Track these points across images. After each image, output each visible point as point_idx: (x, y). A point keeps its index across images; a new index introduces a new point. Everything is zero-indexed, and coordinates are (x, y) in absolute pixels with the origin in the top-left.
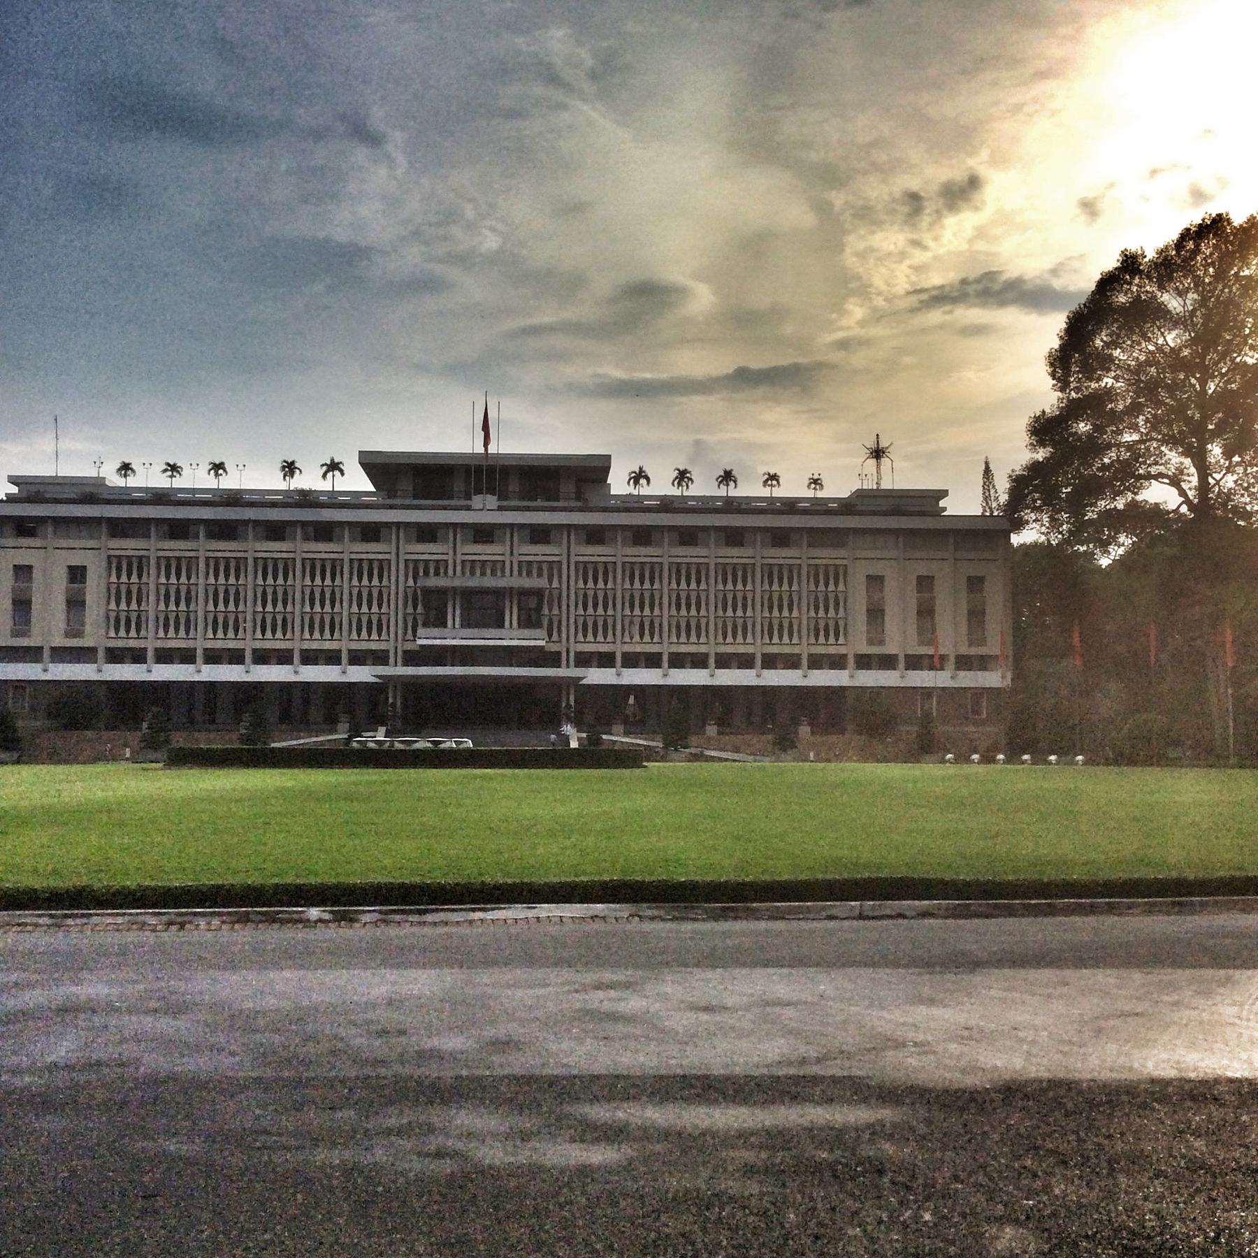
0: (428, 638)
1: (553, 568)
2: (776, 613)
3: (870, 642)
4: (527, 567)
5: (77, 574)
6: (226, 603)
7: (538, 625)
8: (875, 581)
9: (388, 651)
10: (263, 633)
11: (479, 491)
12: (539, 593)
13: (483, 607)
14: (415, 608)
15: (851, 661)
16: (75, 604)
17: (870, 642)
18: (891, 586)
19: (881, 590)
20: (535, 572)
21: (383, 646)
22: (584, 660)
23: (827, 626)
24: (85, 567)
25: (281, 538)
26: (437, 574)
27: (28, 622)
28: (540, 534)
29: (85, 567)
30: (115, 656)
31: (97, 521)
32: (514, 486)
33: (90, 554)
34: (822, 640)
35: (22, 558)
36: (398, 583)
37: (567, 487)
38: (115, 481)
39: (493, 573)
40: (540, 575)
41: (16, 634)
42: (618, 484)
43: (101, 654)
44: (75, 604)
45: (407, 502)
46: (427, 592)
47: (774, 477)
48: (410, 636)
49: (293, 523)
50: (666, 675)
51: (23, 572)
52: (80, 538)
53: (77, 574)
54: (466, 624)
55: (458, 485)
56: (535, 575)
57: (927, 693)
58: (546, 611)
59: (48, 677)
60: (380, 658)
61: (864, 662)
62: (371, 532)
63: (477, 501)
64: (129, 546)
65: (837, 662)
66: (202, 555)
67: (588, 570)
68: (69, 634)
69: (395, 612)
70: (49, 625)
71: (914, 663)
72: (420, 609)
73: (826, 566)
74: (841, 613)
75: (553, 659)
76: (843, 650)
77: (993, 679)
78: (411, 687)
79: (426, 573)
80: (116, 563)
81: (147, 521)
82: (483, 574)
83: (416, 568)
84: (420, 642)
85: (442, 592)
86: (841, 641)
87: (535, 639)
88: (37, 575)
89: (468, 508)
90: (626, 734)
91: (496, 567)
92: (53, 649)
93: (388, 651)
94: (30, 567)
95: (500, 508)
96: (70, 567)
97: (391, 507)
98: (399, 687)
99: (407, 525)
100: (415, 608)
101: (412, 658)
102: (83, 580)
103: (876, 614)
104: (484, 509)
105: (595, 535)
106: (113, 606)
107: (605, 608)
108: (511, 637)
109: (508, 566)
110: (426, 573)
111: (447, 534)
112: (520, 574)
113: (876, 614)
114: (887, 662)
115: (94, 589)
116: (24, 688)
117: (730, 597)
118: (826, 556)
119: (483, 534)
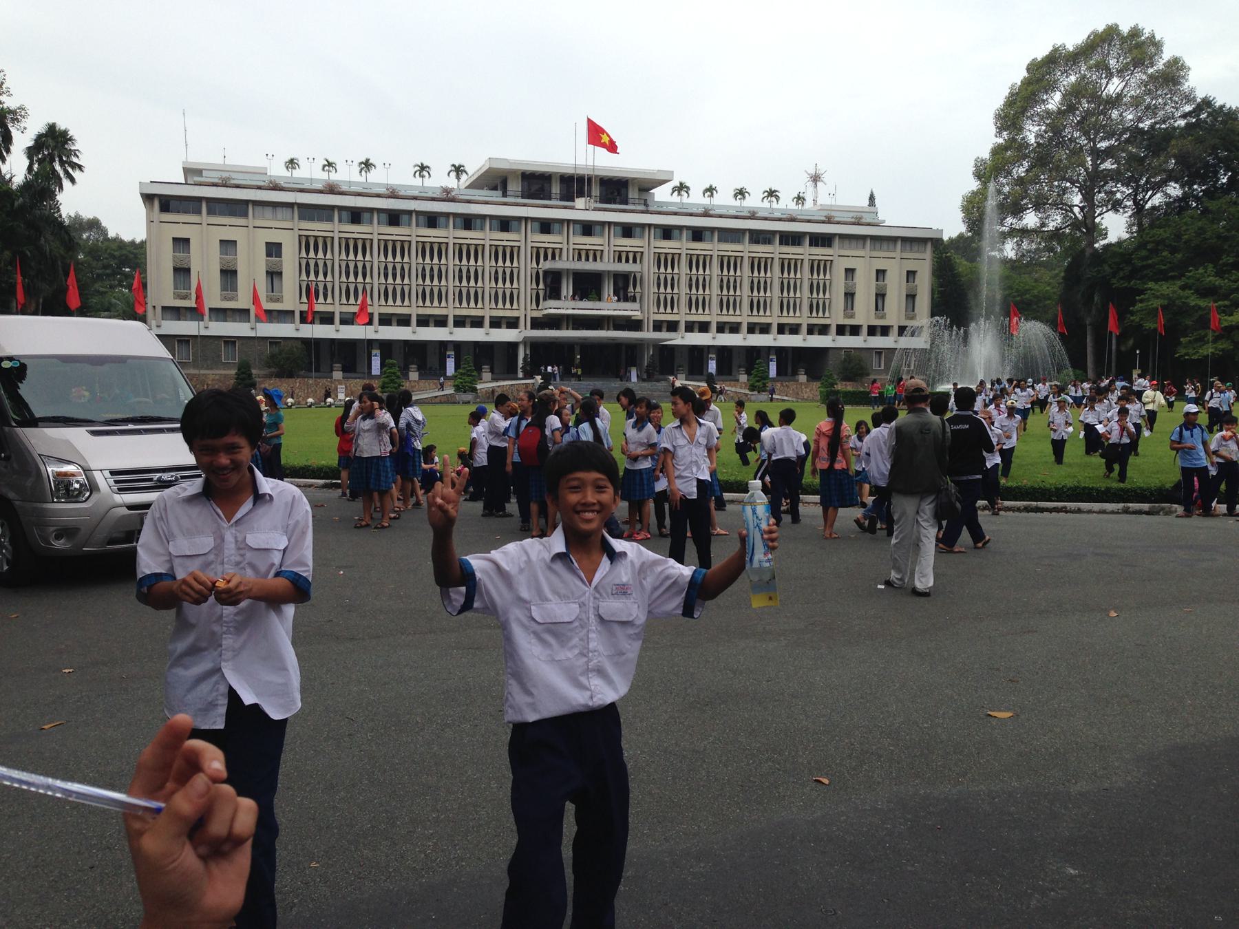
0: (552, 308)
1: (636, 257)
2: (464, 283)
3: (846, 316)
5: (274, 249)
6: (317, 274)
7: (626, 299)
8: (850, 272)
9: (518, 318)
10: (348, 299)
11: (581, 194)
13: (588, 285)
14: (538, 284)
15: (833, 329)
16: (274, 275)
17: (846, 316)
18: (860, 278)
21: (515, 314)
22: (658, 326)
23: (697, 300)
27: (234, 288)
28: (546, 226)
31: (290, 205)
32: (596, 191)
34: (500, 305)
36: (525, 266)
37: (633, 194)
41: (225, 298)
42: (661, 194)
43: (297, 315)
44: (274, 275)
46: (546, 273)
47: (772, 193)
48: (534, 306)
51: (228, 245)
53: (274, 249)
55: (556, 189)
57: (879, 352)
58: (631, 289)
60: (513, 323)
61: (841, 330)
62: (505, 224)
63: (580, 203)
64: (317, 228)
65: (824, 330)
66: (777, 257)
67: (662, 260)
69: (525, 287)
71: (872, 331)
72: (541, 286)
74: (827, 296)
76: (827, 322)
79: (546, 258)
80: (307, 243)
81: (199, 200)
83: (538, 254)
84: (546, 312)
86: (827, 315)
87: (629, 310)
89: (572, 208)
90: (494, 380)
91: (596, 255)
93: (518, 318)
94: (235, 242)
95: (595, 209)
97: (505, 204)
100: (538, 284)
101: (536, 324)
103: (850, 296)
104: (582, 210)
105: (667, 232)
106: (304, 277)
107: (364, 277)
108: (609, 306)
109: (606, 256)
110: (546, 258)
111: (410, 219)
112: (587, 259)
113: (850, 296)
114: (855, 330)
115: (290, 261)
118: (820, 252)
119: (588, 228)
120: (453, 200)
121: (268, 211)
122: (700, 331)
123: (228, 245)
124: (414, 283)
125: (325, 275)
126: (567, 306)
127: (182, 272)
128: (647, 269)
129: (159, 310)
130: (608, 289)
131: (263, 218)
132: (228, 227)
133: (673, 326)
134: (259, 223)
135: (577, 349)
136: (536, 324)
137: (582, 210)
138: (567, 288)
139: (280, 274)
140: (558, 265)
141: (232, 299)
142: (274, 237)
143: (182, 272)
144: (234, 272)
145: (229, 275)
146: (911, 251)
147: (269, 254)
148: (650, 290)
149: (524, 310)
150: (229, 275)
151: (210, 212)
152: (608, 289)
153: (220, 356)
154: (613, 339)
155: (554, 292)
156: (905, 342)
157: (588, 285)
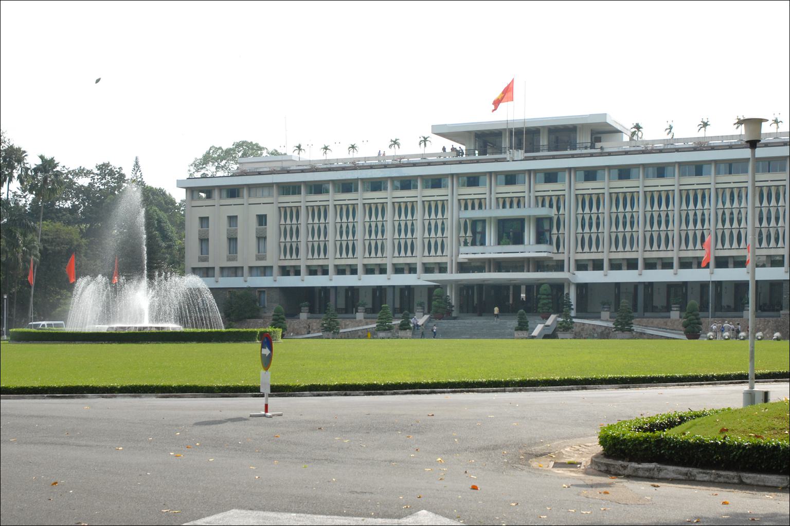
1: (557, 202)
4: (541, 201)
5: (262, 219)
12: (551, 219)
16: (261, 238)
19: (208, 227)
21: (443, 260)
22: (581, 266)
24: (265, 216)
26: (480, 207)
27: (236, 253)
29: (265, 216)
30: (285, 271)
31: (269, 186)
33: (269, 206)
35: (233, 211)
36: (453, 215)
38: (390, 152)
39: (519, 206)
40: (551, 206)
41: (229, 259)
43: (276, 270)
44: (261, 238)
45: (589, 151)
46: (475, 222)
49: (386, 179)
50: (217, 282)
51: (232, 219)
53: (262, 219)
54: (499, 242)
56: (501, 207)
58: (555, 231)
64: (290, 200)
68: (259, 258)
69: (451, 235)
70: (247, 255)
72: (469, 233)
73: (769, 187)
75: (559, 266)
78: (465, 289)
82: (466, 208)
83: (466, 205)
85: (483, 221)
94: (236, 217)
95: (526, 159)
98: (453, 285)
99: (458, 175)
102: (266, 225)
105: (590, 174)
108: (530, 249)
117: (691, 214)
119: (511, 178)
120: (429, 164)
121: (259, 191)
122: (628, 269)
123: (232, 219)
124: (640, 230)
125: (739, 222)
126: (492, 250)
127: (204, 241)
128: (570, 212)
129: (190, 270)
130: (530, 234)
131: (256, 196)
132: (233, 207)
133: (597, 265)
134: (252, 200)
135: (523, 288)
136: (463, 267)
137: (515, 161)
138: (491, 235)
139: (265, 238)
140: (477, 214)
141: (234, 259)
142: (261, 210)
143: (204, 241)
144: (236, 239)
145: (232, 240)
146: (263, 196)
148: (570, 232)
150: (232, 240)
151: (718, 173)
152: (530, 234)
154: (484, 280)
155: (478, 239)
157: (510, 231)
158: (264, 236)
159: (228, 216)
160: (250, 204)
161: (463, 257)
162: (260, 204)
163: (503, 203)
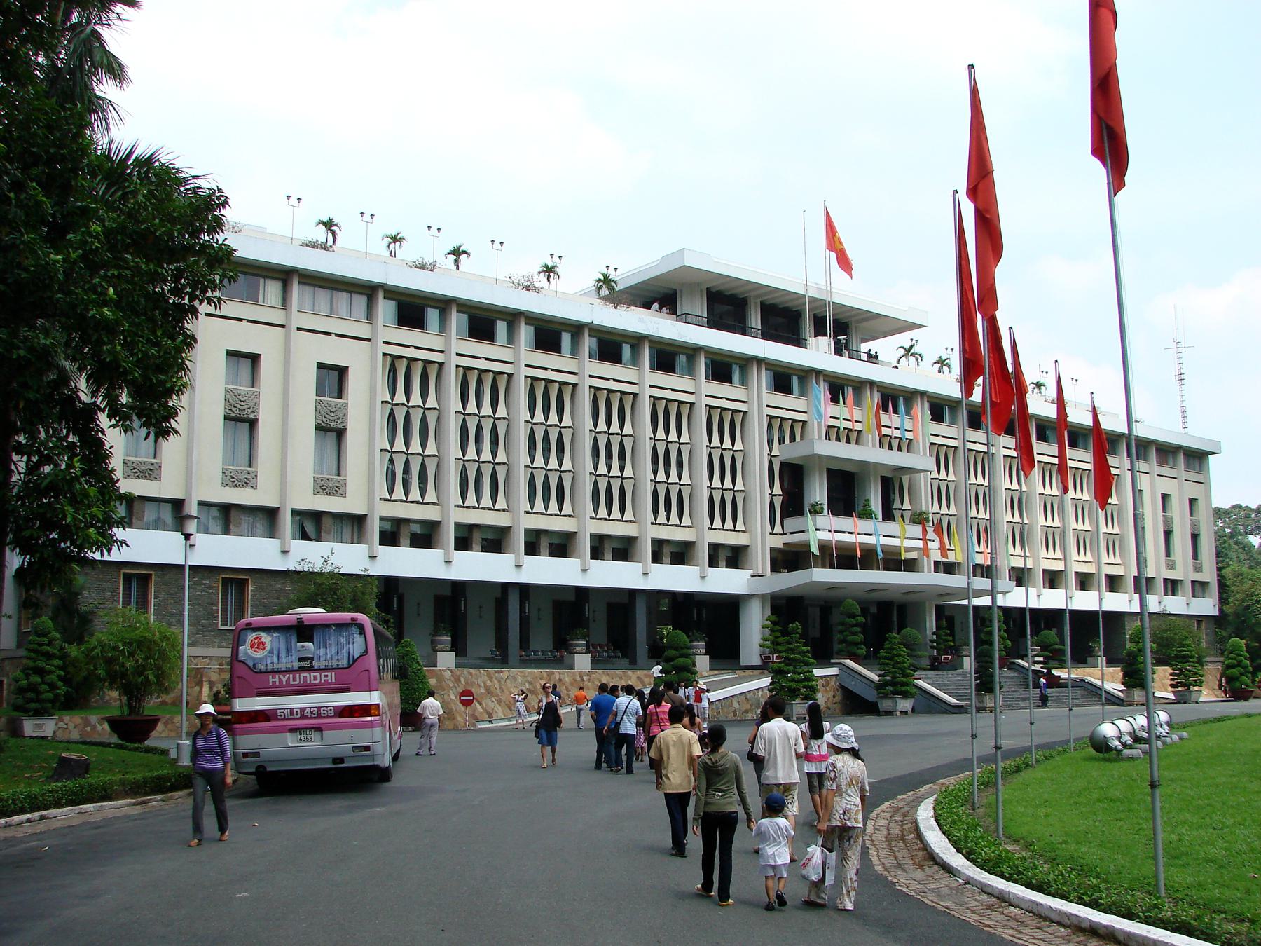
5: (333, 378)
13: (846, 491)
16: (332, 432)
20: (904, 448)
24: (342, 371)
25: (616, 358)
29: (342, 371)
33: (365, 345)
41: (232, 480)
44: (332, 432)
52: (332, 313)
53: (333, 378)
58: (897, 505)
59: (290, 564)
77: (1207, 606)
80: (398, 370)
88: (267, 368)
92: (295, 512)
96: (320, 366)
116: (242, 584)
121: (323, 296)
141: (247, 482)
142: (335, 353)
144: (252, 423)
147: (320, 391)
149: (762, 537)
153: (212, 615)
156: (1176, 605)
158: (341, 426)
159: (230, 354)
160: (369, 340)
161: (778, 542)
162: (329, 334)
163: (834, 433)
